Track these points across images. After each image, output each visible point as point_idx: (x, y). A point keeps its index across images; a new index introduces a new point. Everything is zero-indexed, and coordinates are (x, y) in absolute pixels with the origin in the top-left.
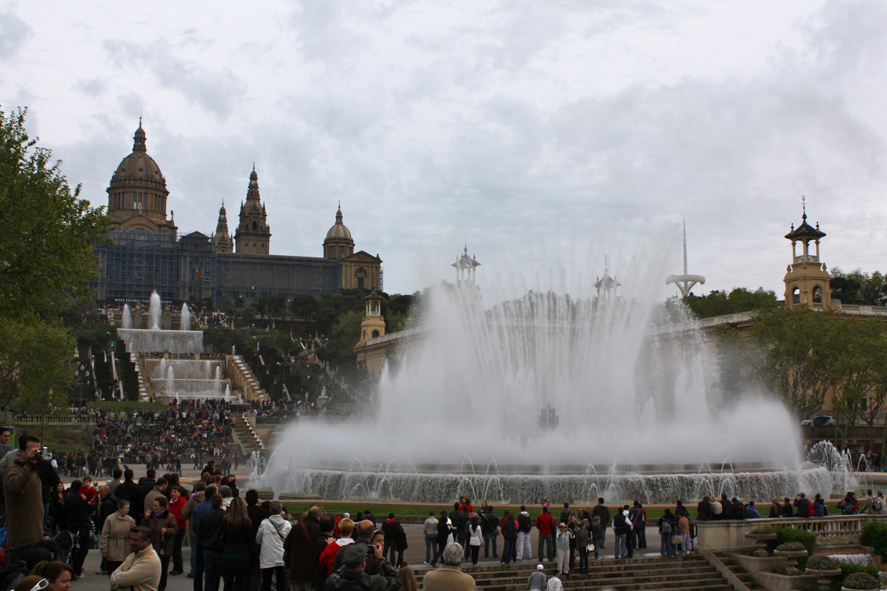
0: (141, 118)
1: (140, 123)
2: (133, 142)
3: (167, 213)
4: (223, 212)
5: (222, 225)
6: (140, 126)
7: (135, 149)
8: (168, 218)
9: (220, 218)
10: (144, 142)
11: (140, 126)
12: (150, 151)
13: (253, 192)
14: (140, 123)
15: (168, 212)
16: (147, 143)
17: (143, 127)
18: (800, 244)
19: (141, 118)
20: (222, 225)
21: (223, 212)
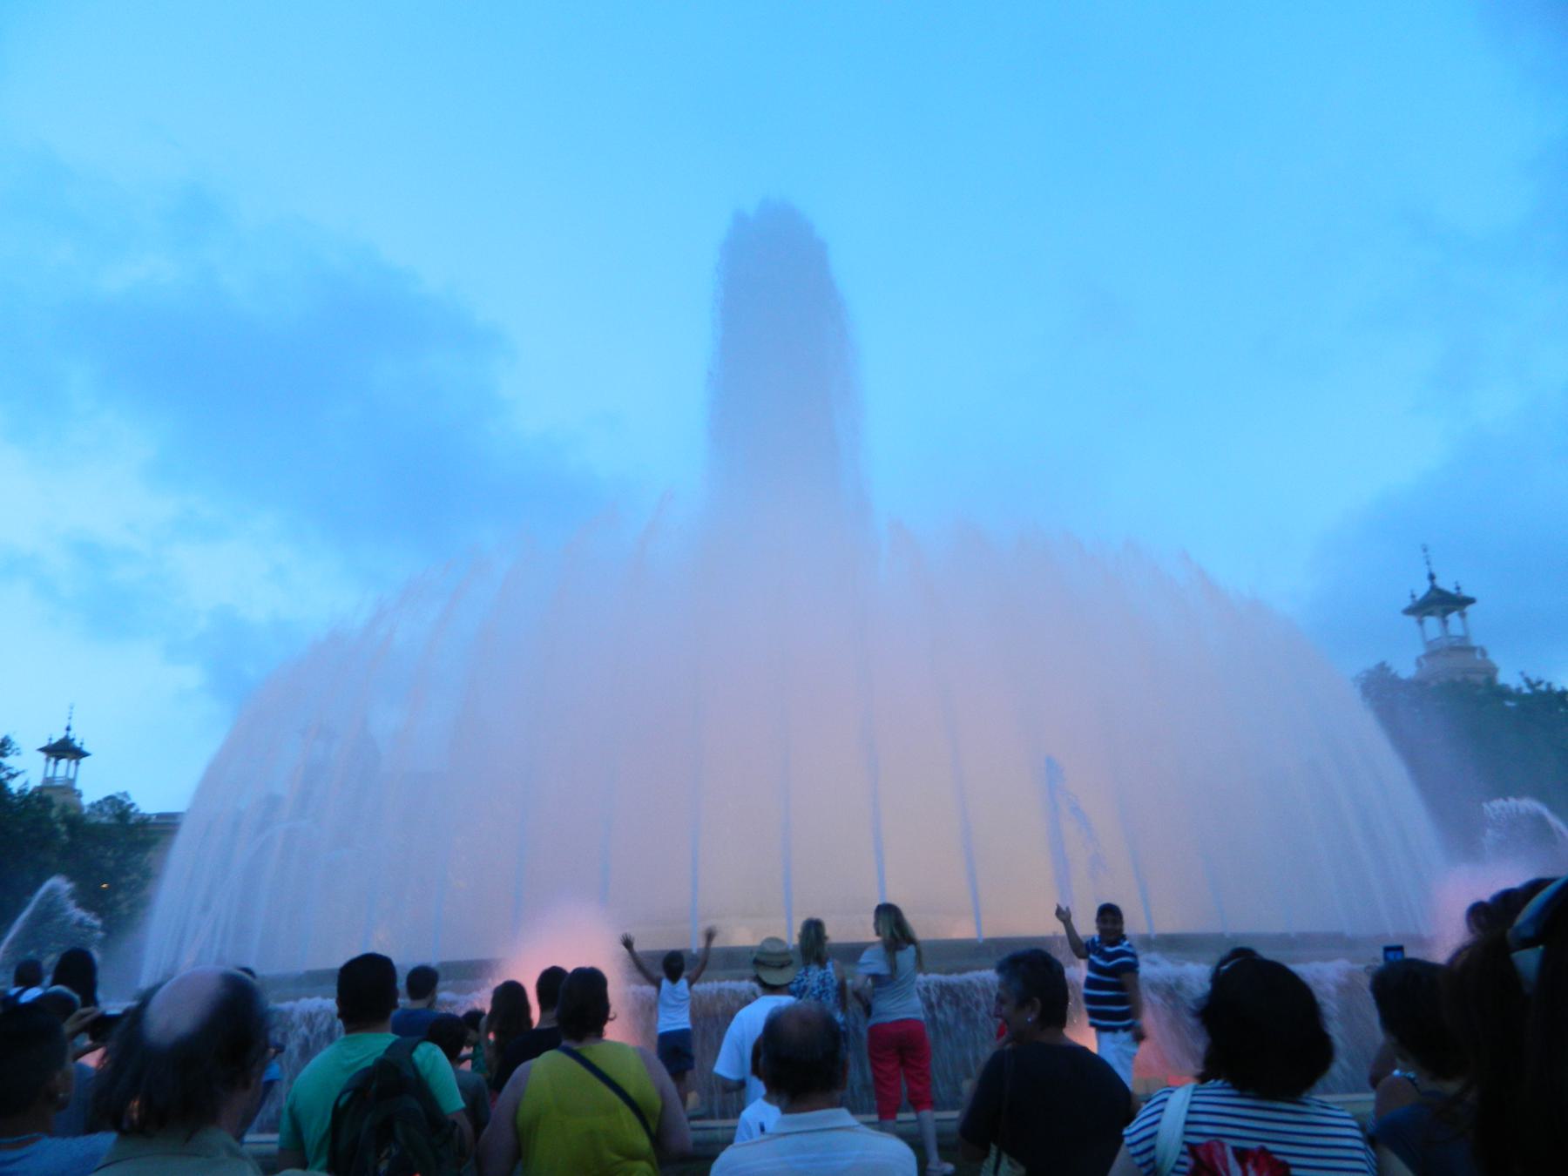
18: (1432, 623)
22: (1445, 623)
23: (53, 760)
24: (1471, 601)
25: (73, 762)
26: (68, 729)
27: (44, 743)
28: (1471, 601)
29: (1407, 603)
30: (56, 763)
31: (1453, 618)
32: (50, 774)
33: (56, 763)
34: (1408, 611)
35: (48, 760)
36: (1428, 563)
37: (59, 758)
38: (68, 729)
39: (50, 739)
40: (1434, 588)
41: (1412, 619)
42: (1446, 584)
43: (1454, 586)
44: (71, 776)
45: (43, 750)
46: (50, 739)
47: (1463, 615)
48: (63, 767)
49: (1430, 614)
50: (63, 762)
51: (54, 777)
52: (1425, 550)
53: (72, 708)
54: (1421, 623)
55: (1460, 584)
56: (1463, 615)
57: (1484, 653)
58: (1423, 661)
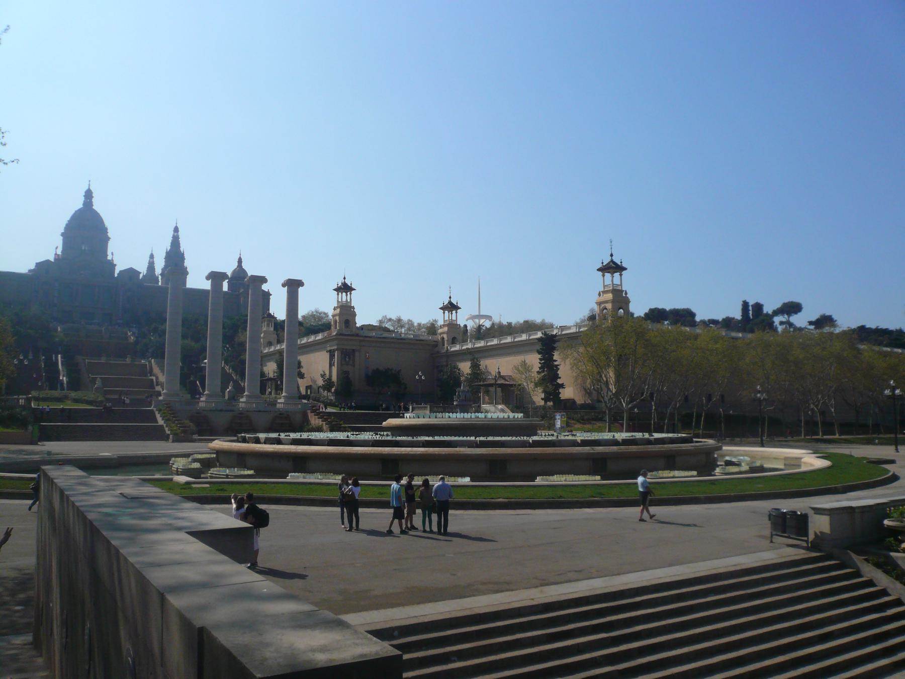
0: (90, 181)
1: (89, 185)
2: (83, 199)
3: (108, 254)
4: (152, 256)
5: (151, 267)
6: (89, 187)
7: (85, 204)
8: (109, 258)
9: (150, 261)
10: (92, 199)
11: (89, 187)
12: (96, 207)
13: (176, 242)
14: (89, 185)
15: (109, 253)
16: (93, 200)
17: (91, 188)
18: (608, 275)
19: (90, 181)
20: (151, 267)
21: (152, 256)
22: (613, 277)
24: (625, 269)
28: (625, 269)
29: (600, 266)
31: (617, 275)
34: (599, 270)
36: (611, 249)
40: (612, 261)
41: (600, 273)
42: (617, 260)
43: (620, 261)
47: (621, 275)
49: (609, 272)
52: (611, 242)
54: (604, 276)
55: (622, 261)
56: (621, 275)
57: (626, 293)
58: (601, 293)
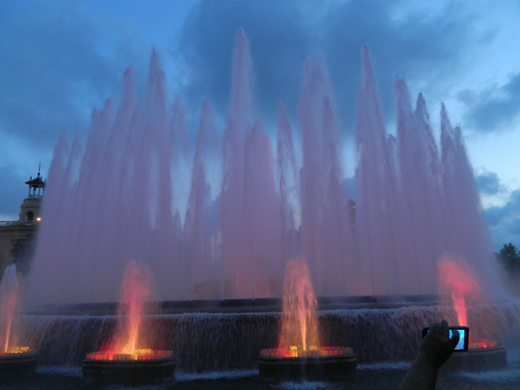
23: (33, 188)
25: (42, 189)
26: (39, 174)
27: (28, 180)
30: (35, 190)
32: (32, 193)
33: (35, 190)
35: (30, 188)
37: (35, 187)
38: (39, 174)
39: (31, 178)
44: (41, 194)
45: (27, 183)
46: (31, 178)
48: (39, 191)
50: (37, 189)
51: (34, 195)
53: (40, 165)
